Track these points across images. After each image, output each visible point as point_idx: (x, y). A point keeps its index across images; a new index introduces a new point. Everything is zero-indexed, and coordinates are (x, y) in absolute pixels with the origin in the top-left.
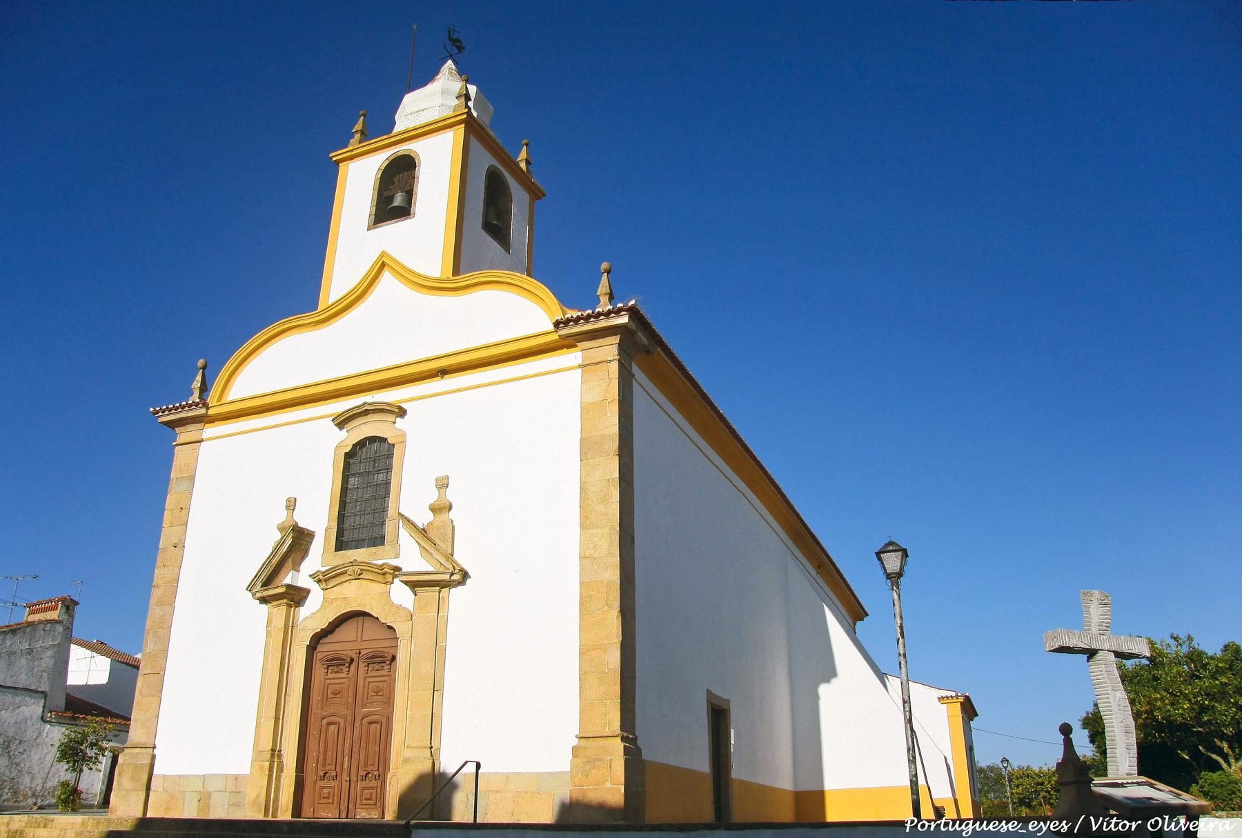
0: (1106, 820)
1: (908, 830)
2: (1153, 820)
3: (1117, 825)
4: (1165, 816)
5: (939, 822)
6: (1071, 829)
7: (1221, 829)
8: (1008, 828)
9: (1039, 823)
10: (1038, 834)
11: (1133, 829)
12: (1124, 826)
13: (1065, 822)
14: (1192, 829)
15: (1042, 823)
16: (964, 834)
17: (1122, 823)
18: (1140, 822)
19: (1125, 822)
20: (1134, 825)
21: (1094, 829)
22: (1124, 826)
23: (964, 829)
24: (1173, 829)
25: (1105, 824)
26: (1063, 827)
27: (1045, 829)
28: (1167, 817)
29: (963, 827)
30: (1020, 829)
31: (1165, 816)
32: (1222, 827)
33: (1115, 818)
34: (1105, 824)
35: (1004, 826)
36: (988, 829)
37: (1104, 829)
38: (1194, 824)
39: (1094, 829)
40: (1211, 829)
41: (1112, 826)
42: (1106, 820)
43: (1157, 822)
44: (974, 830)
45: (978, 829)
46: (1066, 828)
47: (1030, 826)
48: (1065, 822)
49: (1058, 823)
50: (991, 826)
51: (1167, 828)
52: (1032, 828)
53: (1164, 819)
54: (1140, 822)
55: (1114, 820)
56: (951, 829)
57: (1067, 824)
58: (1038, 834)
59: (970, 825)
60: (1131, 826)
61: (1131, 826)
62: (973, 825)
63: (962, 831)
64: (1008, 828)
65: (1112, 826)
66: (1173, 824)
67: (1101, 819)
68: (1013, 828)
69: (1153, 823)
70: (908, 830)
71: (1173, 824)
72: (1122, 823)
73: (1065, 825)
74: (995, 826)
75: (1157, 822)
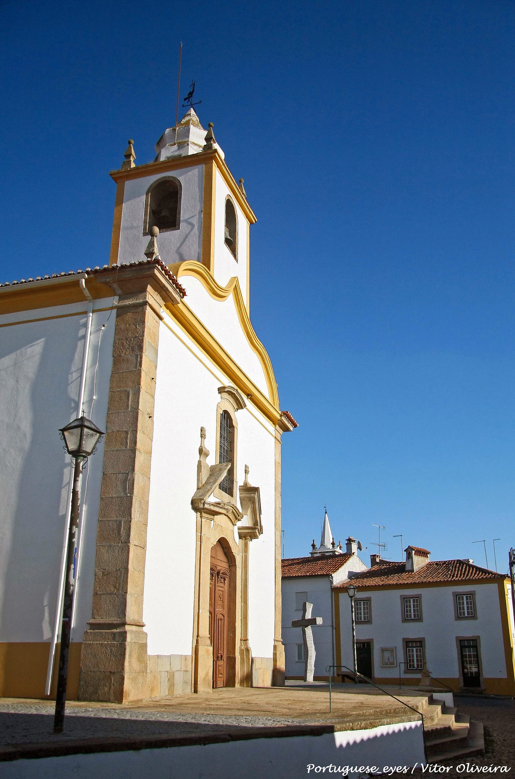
0: (431, 766)
1: (308, 772)
2: (460, 766)
3: (437, 769)
4: (467, 763)
5: (328, 767)
6: (410, 771)
7: (501, 771)
8: (370, 771)
9: (389, 768)
10: (389, 775)
11: (324, 771)
12: (442, 769)
13: (405, 767)
14: (398, 771)
15: (391, 768)
16: (343, 774)
17: (441, 767)
18: (452, 767)
19: (443, 767)
20: (448, 769)
21: (424, 771)
22: (442, 769)
23: (343, 771)
24: (506, 771)
25: (430, 768)
26: (404, 770)
27: (393, 771)
28: (468, 764)
29: (343, 770)
30: (377, 771)
31: (467, 763)
32: (503, 770)
33: (436, 765)
34: (430, 768)
35: (368, 769)
36: (358, 771)
37: (430, 771)
38: (485, 768)
39: (424, 771)
40: (495, 772)
41: (435, 769)
42: (431, 766)
43: (462, 767)
44: (350, 772)
45: (352, 771)
46: (406, 771)
47: (384, 769)
48: (405, 767)
49: (364, 768)
50: (360, 770)
51: (469, 771)
52: (386, 771)
53: (466, 766)
54: (452, 767)
55: (436, 766)
56: (335, 771)
57: (406, 769)
58: (389, 775)
59: (347, 769)
60: (322, 770)
61: (446, 770)
62: (349, 769)
63: (342, 772)
64: (370, 771)
65: (435, 769)
66: (472, 768)
67: (428, 765)
68: (373, 771)
69: (460, 768)
70: (308, 772)
71: (472, 768)
72: (441, 767)
73: (405, 769)
74: (374, 769)
75: (462, 767)
